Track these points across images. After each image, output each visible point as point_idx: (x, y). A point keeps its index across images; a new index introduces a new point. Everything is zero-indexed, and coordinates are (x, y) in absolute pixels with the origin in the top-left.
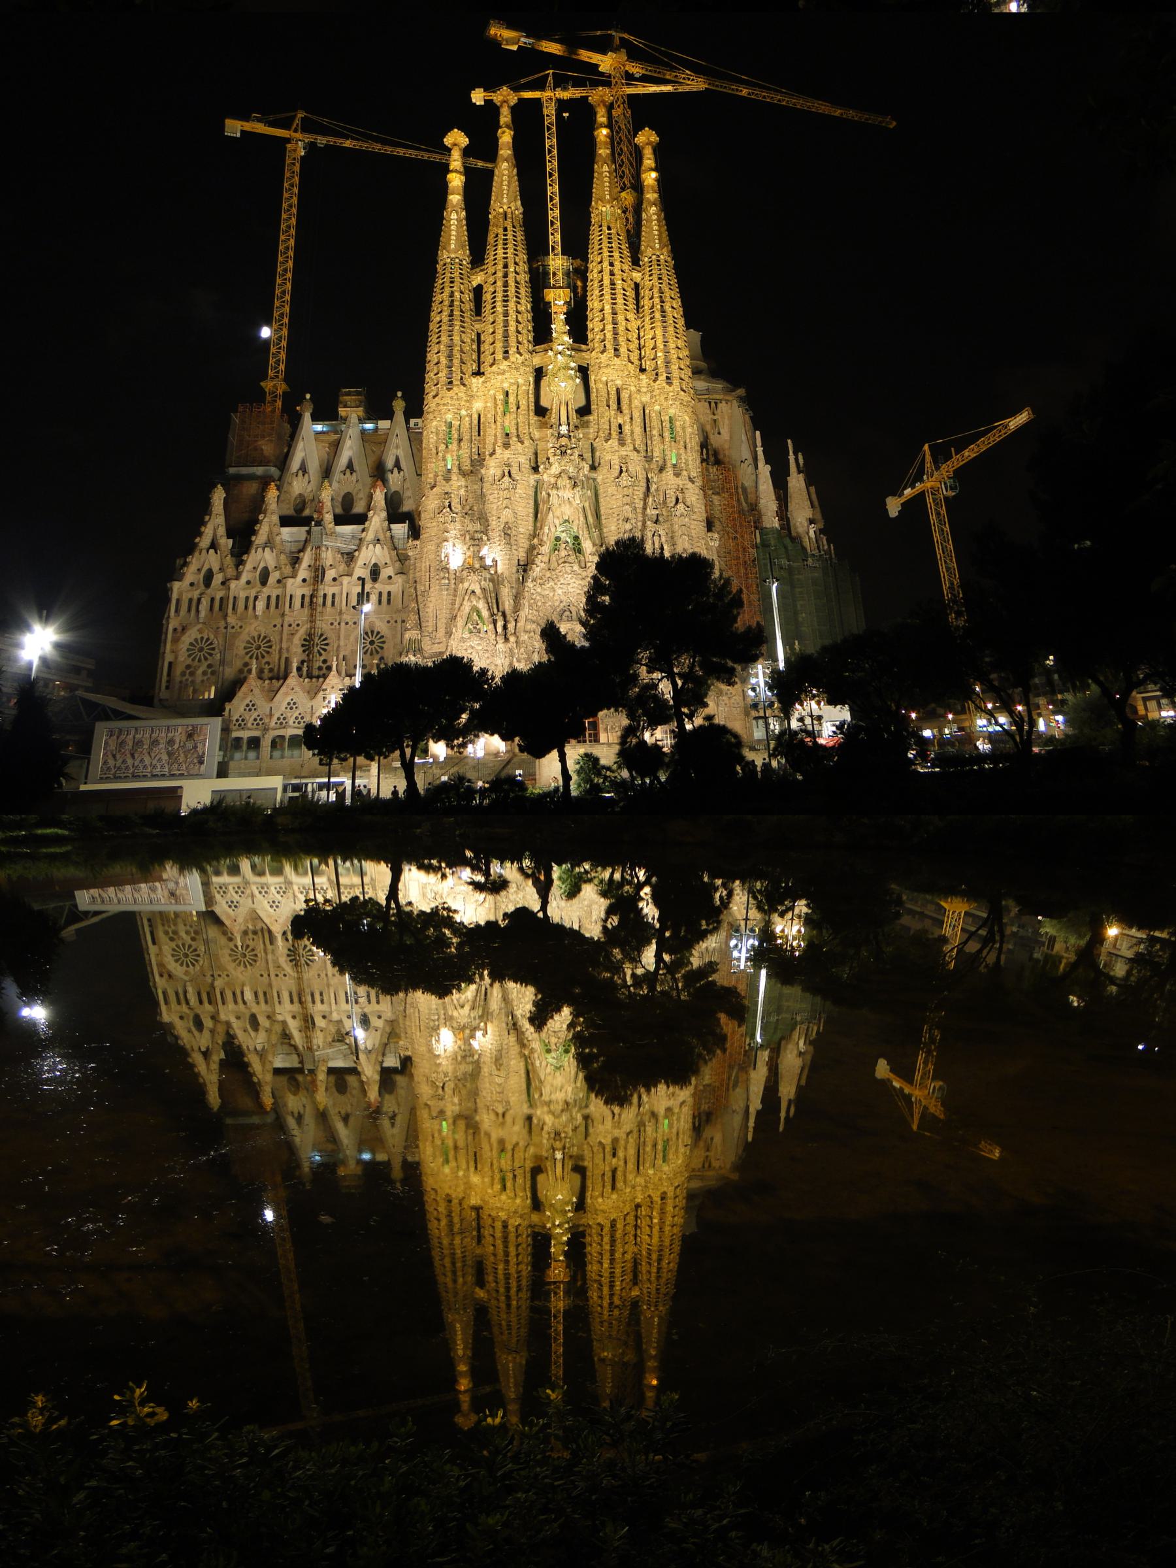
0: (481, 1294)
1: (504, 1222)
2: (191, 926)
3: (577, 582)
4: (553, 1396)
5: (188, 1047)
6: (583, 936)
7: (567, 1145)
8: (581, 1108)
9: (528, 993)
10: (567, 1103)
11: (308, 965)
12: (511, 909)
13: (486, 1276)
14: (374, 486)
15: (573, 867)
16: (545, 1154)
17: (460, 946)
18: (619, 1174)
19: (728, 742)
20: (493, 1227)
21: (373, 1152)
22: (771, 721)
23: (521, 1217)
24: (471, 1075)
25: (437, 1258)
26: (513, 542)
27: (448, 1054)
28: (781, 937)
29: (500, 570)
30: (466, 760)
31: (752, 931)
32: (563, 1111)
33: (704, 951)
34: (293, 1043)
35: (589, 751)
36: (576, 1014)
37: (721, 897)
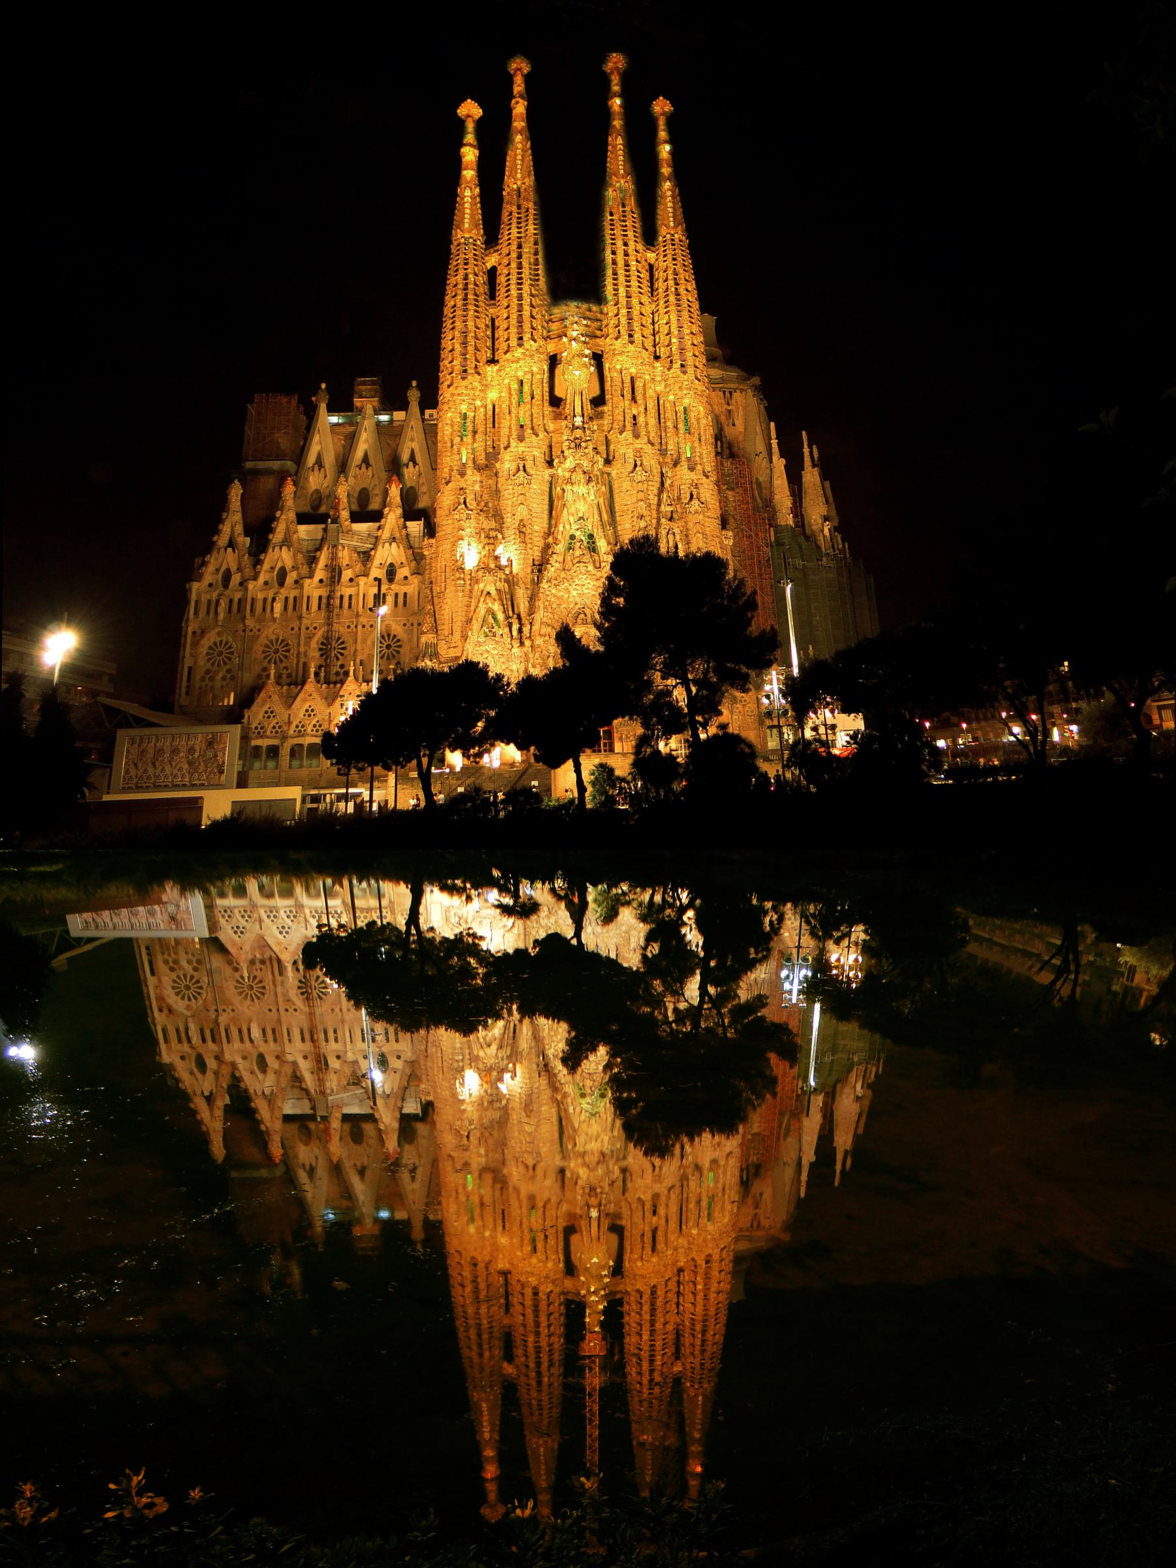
0: (509, 1369)
1: (534, 1288)
2: (193, 955)
3: (592, 583)
4: (588, 1485)
5: (190, 1091)
6: (620, 966)
7: (603, 1202)
8: (618, 1160)
9: (560, 1030)
10: (603, 1154)
11: (320, 998)
12: (542, 935)
13: (515, 1350)
14: (389, 481)
15: (610, 888)
16: (578, 1211)
17: (486, 977)
18: (660, 1234)
19: (742, 751)
20: (523, 1294)
21: (392, 1209)
22: (785, 730)
23: (553, 1282)
24: (499, 1123)
25: (462, 1329)
26: (528, 541)
27: (473, 1099)
28: (836, 967)
29: (515, 571)
30: (482, 771)
31: (805, 960)
32: (598, 1163)
33: (753, 983)
34: (304, 1086)
35: (604, 761)
36: (613, 1054)
37: (771, 922)
